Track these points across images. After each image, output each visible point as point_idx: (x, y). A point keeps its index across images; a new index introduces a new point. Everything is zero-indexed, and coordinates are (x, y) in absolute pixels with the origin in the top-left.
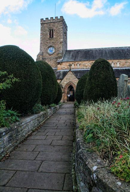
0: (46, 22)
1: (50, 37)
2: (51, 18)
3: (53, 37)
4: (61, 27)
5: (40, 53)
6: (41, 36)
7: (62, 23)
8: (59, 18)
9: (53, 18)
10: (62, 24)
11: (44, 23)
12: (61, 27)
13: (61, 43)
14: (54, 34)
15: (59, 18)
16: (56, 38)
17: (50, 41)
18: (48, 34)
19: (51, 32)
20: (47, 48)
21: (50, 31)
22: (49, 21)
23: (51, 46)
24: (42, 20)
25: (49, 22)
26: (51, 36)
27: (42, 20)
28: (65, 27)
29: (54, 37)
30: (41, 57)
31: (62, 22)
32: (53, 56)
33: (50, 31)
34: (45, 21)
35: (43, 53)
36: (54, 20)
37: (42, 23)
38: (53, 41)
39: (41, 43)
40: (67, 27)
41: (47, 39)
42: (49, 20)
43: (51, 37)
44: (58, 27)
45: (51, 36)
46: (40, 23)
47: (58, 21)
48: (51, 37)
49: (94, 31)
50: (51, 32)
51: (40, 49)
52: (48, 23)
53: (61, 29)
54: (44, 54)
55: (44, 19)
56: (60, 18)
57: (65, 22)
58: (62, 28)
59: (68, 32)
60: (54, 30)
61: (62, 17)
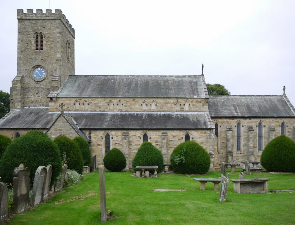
0: (28, 18)
1: (37, 49)
2: (38, 10)
3: (42, 48)
4: (58, 30)
5: (16, 77)
6: (18, 43)
7: (59, 23)
8: (53, 12)
9: (41, 10)
10: (58, 25)
11: (24, 18)
12: (58, 30)
13: (57, 61)
14: (44, 42)
15: (53, 12)
16: (47, 52)
17: (36, 56)
18: (33, 42)
19: (39, 38)
20: (31, 68)
21: (37, 36)
22: (34, 15)
23: (39, 66)
24: (20, 11)
25: (34, 18)
26: (39, 46)
27: (20, 11)
28: (69, 31)
29: (45, 48)
30: (19, 84)
31: (59, 21)
32: (43, 85)
33: (37, 36)
34: (25, 14)
35: (23, 77)
36: (44, 15)
37: (19, 17)
38: (41, 56)
39: (19, 59)
40: (73, 31)
41: (31, 51)
42: (35, 14)
43: (39, 47)
44: (53, 32)
45: (39, 46)
46: (16, 17)
47: (52, 18)
48: (39, 47)
49: (251, 71)
50: (39, 38)
51: (18, 70)
52: (33, 19)
53: (58, 35)
54: (26, 80)
55: (25, 11)
56: (54, 12)
57: (67, 21)
58: (60, 33)
59: (76, 41)
60: (45, 36)
61: (58, 11)
